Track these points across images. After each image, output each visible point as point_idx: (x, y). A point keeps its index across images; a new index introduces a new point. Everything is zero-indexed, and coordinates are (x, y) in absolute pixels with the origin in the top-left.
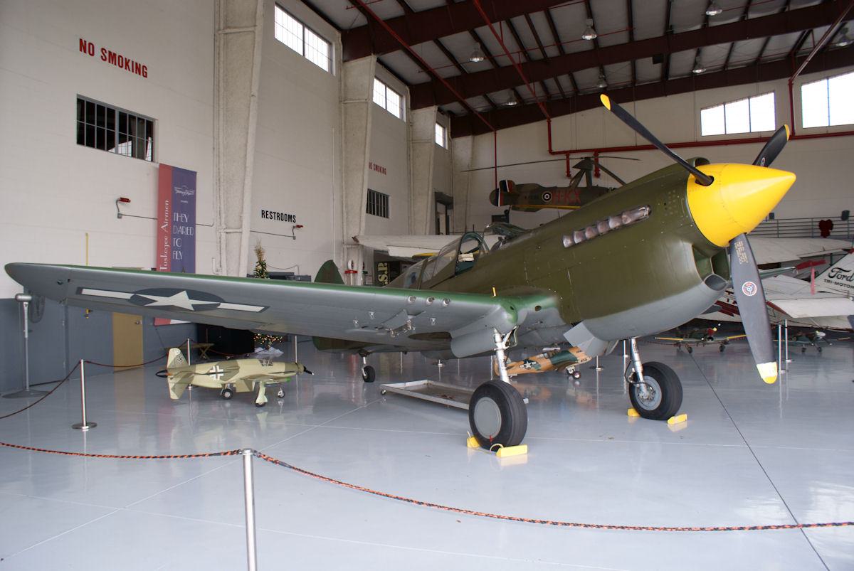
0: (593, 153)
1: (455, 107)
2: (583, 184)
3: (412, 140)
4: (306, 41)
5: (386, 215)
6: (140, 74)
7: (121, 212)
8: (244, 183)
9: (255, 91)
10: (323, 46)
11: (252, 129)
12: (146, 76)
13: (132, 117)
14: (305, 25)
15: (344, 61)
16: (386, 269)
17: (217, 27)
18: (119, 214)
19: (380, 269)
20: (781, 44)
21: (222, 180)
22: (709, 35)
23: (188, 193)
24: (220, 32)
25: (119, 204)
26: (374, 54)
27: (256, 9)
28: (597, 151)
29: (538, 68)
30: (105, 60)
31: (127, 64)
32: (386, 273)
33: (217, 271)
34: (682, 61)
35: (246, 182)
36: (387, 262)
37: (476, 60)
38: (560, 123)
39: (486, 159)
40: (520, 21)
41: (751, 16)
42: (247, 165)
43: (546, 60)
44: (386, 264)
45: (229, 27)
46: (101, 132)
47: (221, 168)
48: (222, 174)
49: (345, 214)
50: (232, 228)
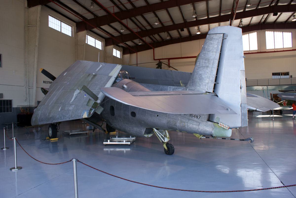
3: (106, 56)
4: (62, 26)
14: (61, 21)
15: (77, 32)
17: (25, 24)
24: (26, 26)
28: (169, 59)
29: (144, 33)
33: (26, 100)
39: (134, 61)
41: (222, 14)
43: (147, 30)
45: (29, 24)
47: (27, 69)
48: (27, 70)
50: (31, 87)
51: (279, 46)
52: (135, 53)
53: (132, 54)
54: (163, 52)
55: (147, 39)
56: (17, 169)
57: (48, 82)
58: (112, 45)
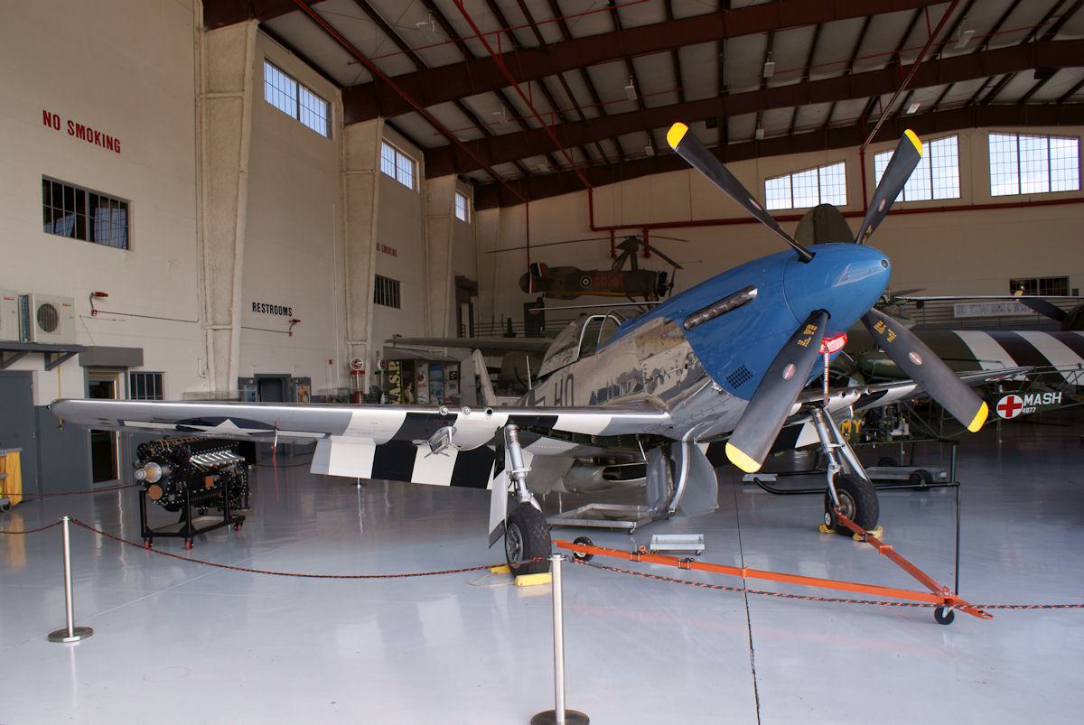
1: (480, 174)
2: (627, 266)
3: (428, 215)
4: (301, 102)
5: (396, 304)
6: (112, 149)
8: (233, 273)
9: (244, 166)
10: (320, 107)
11: (241, 211)
12: (119, 152)
13: (105, 199)
14: (299, 83)
15: (346, 125)
16: (398, 368)
17: (198, 90)
19: (391, 369)
20: (849, 110)
22: (766, 98)
24: (202, 96)
25: (93, 300)
27: (244, 70)
28: (646, 228)
29: (573, 131)
30: (73, 134)
31: (97, 139)
32: (398, 373)
34: (742, 125)
35: (236, 271)
36: (400, 361)
38: (603, 194)
40: (553, 81)
42: (237, 252)
43: (584, 122)
44: (398, 363)
48: (206, 262)
50: (220, 325)
51: (1035, 185)
52: (519, 202)
53: (509, 208)
54: (625, 202)
56: (78, 638)
57: (266, 308)
58: (451, 174)
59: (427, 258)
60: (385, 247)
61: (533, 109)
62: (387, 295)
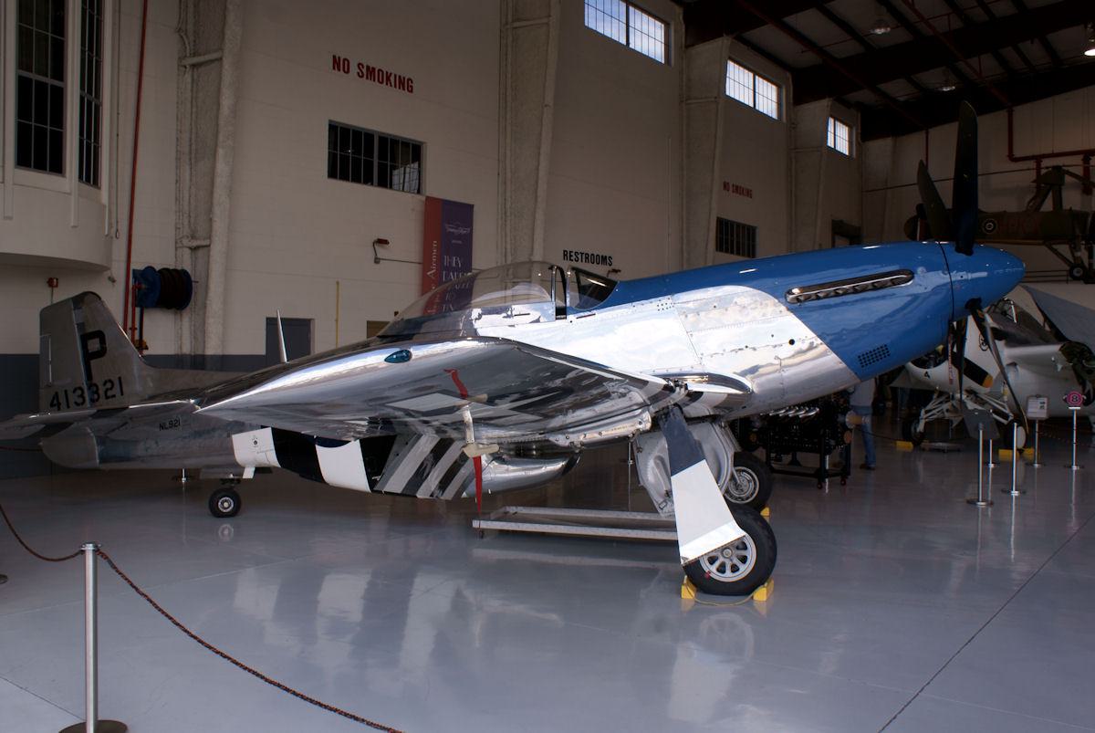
0: (1081, 157)
1: (864, 96)
7: (379, 256)
8: (534, 218)
9: (549, 99)
12: (411, 91)
17: (504, 21)
18: (376, 258)
21: (508, 214)
23: (462, 231)
24: (509, 26)
26: (727, 34)
30: (362, 77)
31: (388, 79)
35: (537, 216)
37: (879, 31)
45: (519, 20)
46: (356, 162)
49: (685, 255)
55: (986, 66)
57: (579, 256)
59: (794, 198)
60: (737, 187)
61: (916, 11)
62: (738, 243)
